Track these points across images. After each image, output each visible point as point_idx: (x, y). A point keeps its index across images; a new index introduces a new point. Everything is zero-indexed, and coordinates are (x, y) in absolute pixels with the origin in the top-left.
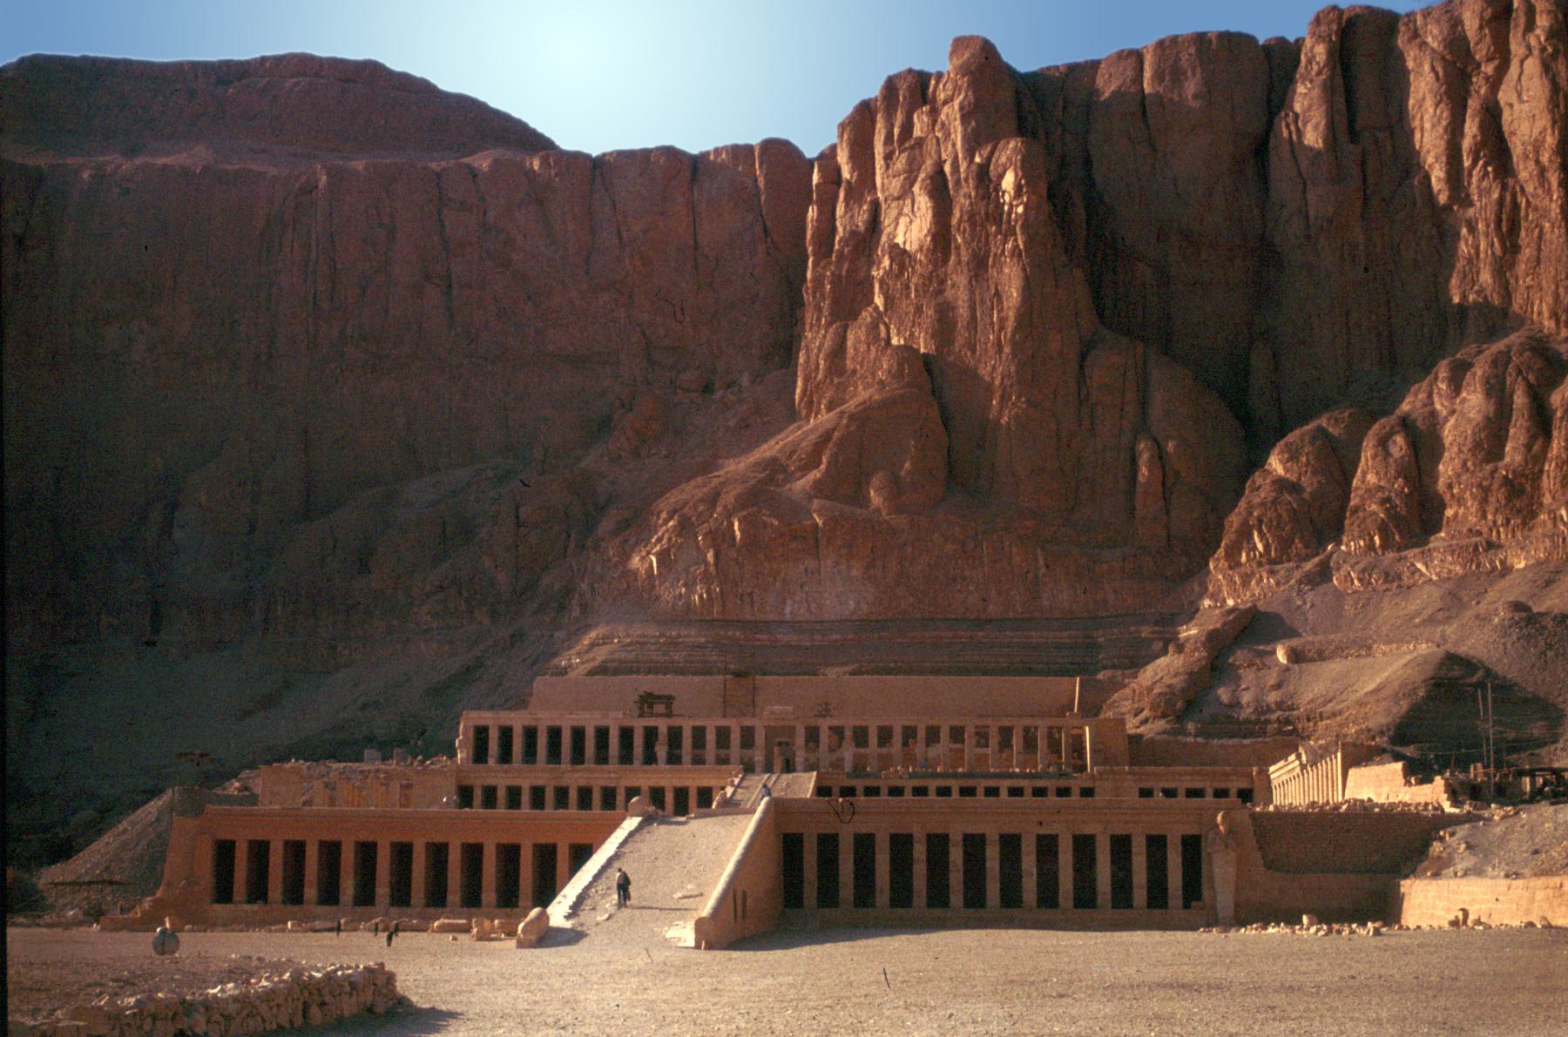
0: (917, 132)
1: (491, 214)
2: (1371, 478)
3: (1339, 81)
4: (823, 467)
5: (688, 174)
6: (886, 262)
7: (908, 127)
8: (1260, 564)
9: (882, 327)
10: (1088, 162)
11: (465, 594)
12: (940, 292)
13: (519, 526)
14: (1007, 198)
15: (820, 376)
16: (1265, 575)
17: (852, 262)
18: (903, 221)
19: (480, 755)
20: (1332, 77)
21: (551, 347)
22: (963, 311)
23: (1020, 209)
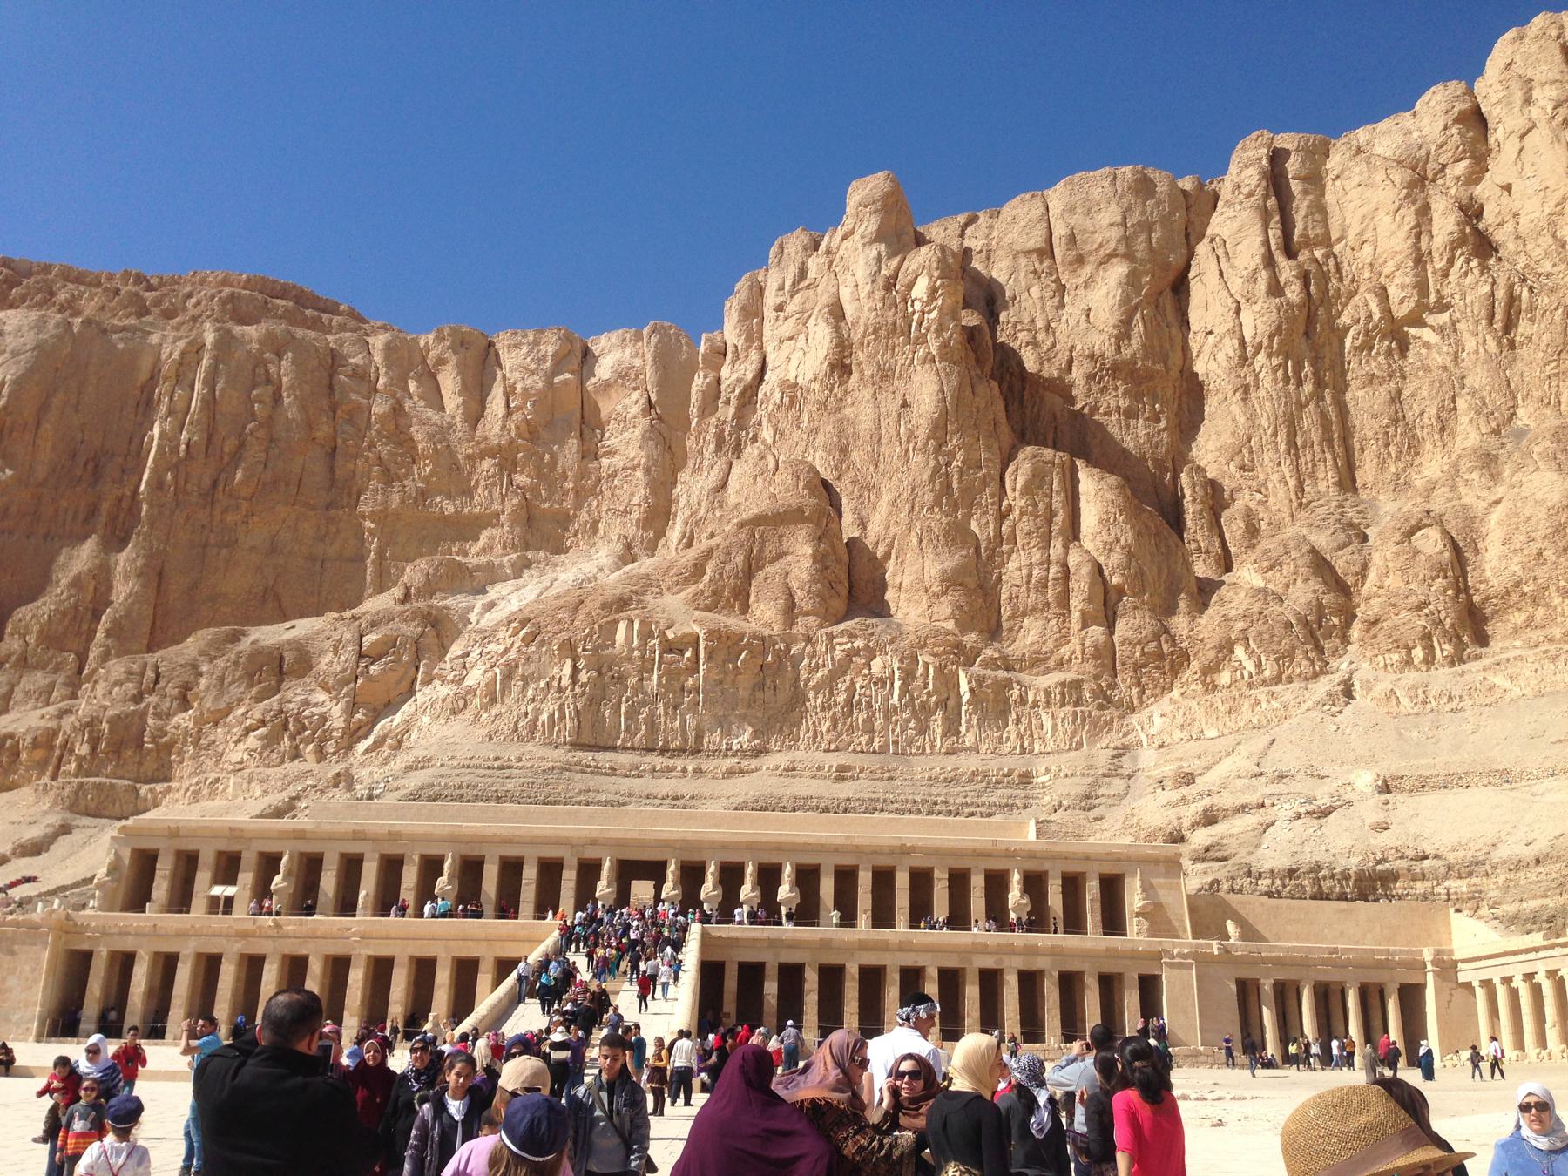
0: (811, 275)
1: (381, 381)
2: (1394, 582)
3: (1272, 202)
4: (706, 578)
5: (579, 354)
6: (777, 395)
7: (803, 273)
8: (1250, 686)
9: (770, 459)
11: (291, 727)
13: (361, 656)
14: (917, 305)
15: (702, 513)
16: (1263, 697)
17: (738, 409)
18: (797, 355)
20: (1266, 197)
22: (866, 424)
23: (934, 314)
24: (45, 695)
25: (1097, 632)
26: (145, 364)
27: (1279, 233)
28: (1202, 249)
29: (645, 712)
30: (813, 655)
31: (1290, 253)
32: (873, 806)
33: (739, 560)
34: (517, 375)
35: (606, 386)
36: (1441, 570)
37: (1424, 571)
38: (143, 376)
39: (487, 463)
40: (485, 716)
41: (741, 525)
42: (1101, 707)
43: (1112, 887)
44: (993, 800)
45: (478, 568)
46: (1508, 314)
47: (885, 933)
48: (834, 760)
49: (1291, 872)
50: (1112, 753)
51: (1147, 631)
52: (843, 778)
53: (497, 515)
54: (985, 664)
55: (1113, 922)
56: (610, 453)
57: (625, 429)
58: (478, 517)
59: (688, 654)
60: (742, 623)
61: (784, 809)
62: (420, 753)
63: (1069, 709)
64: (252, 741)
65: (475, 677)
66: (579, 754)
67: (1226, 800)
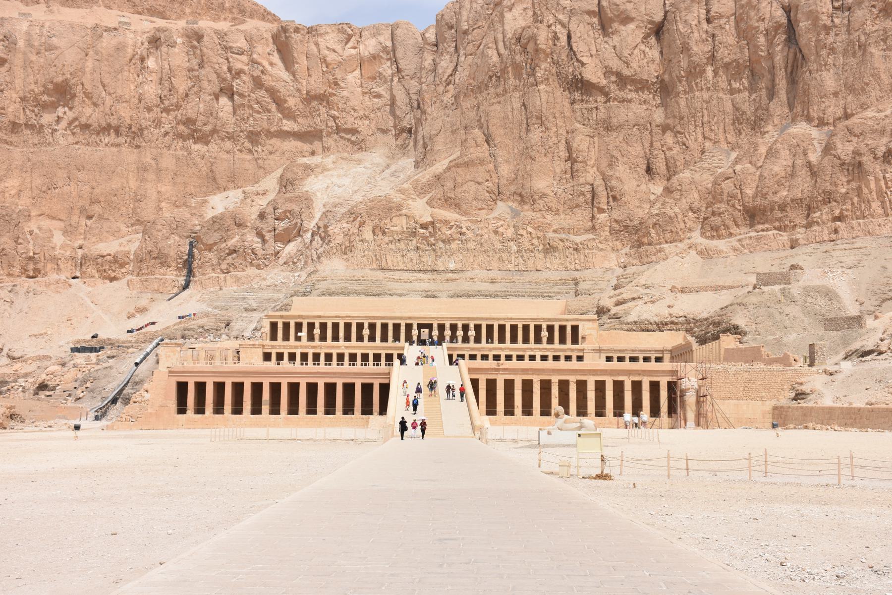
1: (255, 56)
10: (569, 37)
12: (493, 104)
15: (429, 148)
19: (274, 337)
21: (285, 128)
24: (116, 234)
25: (602, 217)
26: (130, 51)
27: (705, 11)
28: (670, 17)
29: (411, 255)
30: (482, 229)
31: (709, 21)
32: (505, 295)
33: (449, 184)
34: (327, 52)
35: (374, 57)
36: (732, 196)
37: (725, 198)
38: (129, 56)
39: (315, 103)
40: (346, 257)
41: (449, 168)
42: (601, 250)
43: (575, 329)
44: (556, 290)
45: (317, 166)
46: (793, 66)
47: (502, 345)
48: (492, 274)
49: (635, 323)
50: (604, 270)
51: (625, 217)
52: (492, 282)
53: (321, 131)
54: (555, 231)
55: (575, 341)
56: (379, 96)
57: (386, 82)
58: (310, 132)
59: (431, 229)
60: (452, 215)
61: (469, 296)
62: (323, 274)
63: (587, 251)
64: (230, 259)
65: (340, 239)
66: (388, 274)
67: (625, 296)
